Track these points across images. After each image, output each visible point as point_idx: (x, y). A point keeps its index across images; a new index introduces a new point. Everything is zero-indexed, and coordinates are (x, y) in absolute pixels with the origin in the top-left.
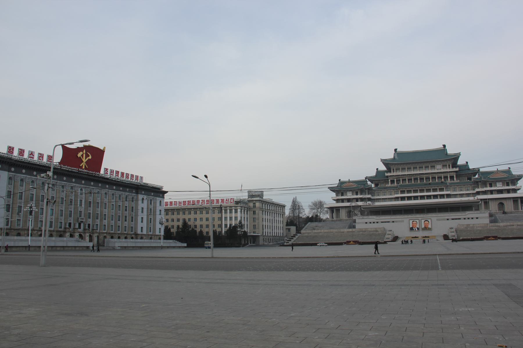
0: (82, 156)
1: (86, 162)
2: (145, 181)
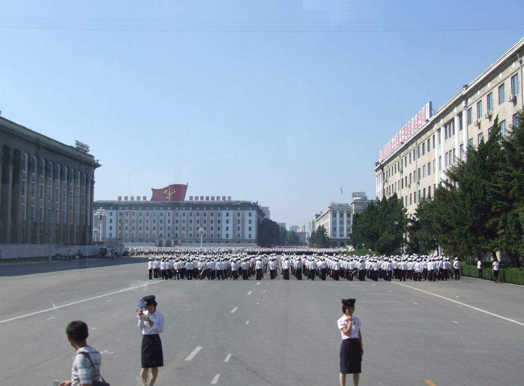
0: (168, 192)
1: (171, 196)
2: (234, 199)
